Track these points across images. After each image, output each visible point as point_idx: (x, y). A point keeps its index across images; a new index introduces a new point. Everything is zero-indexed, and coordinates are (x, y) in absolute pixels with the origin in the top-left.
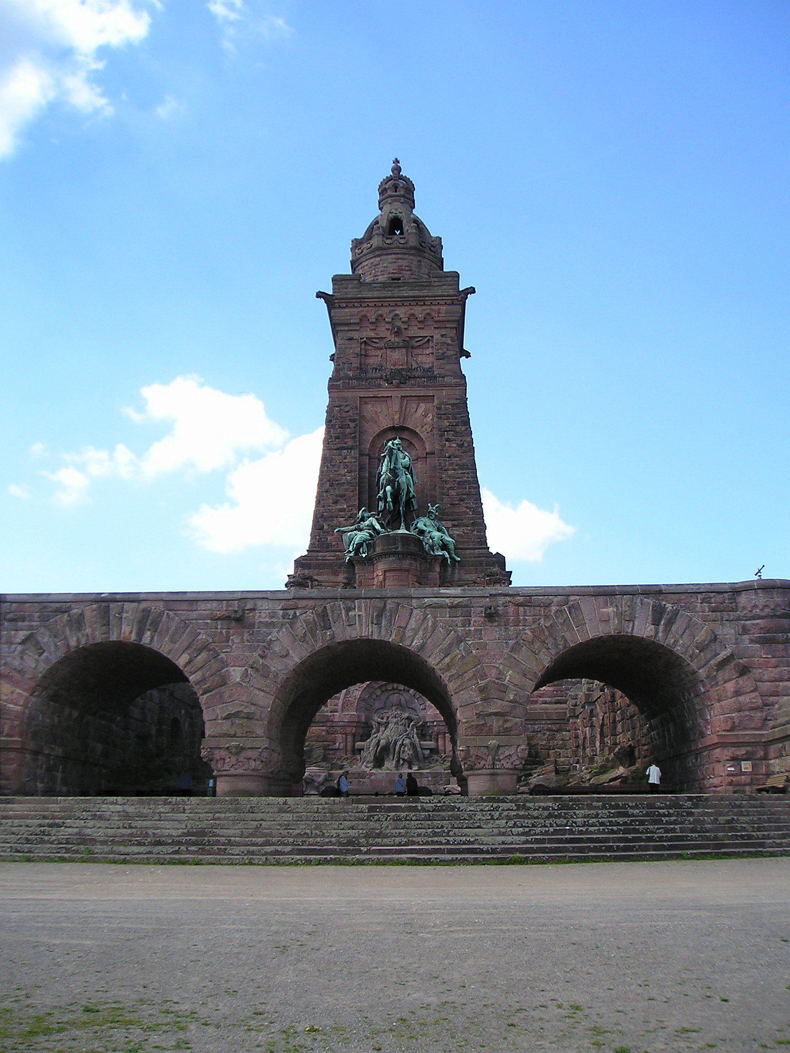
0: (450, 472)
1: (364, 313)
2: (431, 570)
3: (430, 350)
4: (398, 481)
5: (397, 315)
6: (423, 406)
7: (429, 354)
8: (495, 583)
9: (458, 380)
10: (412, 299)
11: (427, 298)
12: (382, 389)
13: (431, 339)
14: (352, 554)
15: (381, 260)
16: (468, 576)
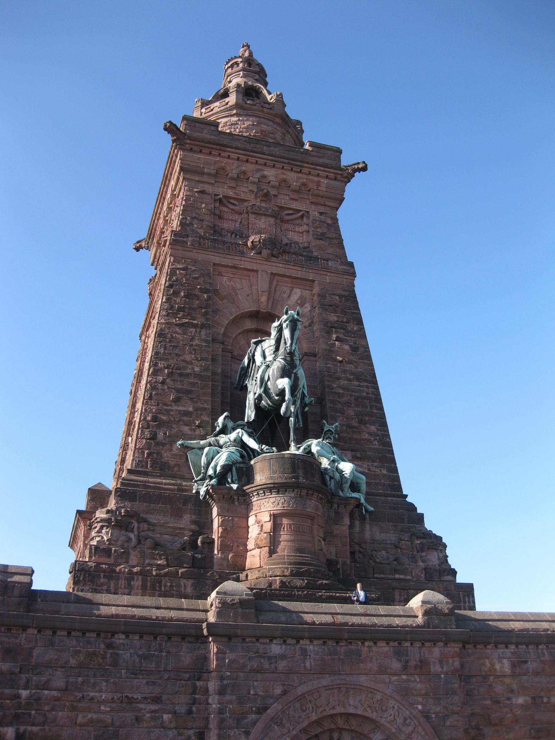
0: (343, 382)
1: (223, 164)
2: (338, 519)
3: (305, 228)
4: (296, 374)
5: (264, 177)
6: (297, 293)
7: (302, 233)
8: (428, 549)
9: (346, 267)
10: (287, 161)
11: (305, 165)
12: (246, 259)
13: (306, 214)
14: (213, 481)
15: (239, 120)
16: (383, 536)
